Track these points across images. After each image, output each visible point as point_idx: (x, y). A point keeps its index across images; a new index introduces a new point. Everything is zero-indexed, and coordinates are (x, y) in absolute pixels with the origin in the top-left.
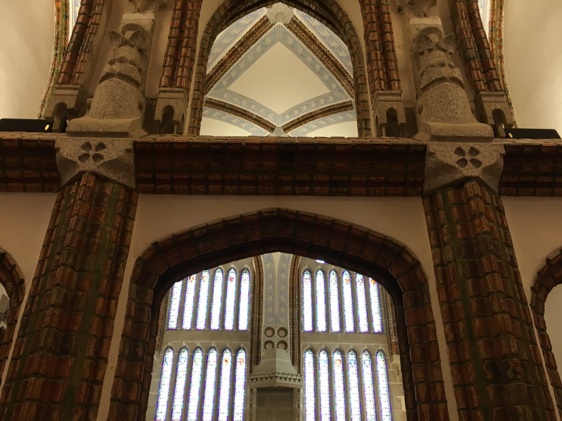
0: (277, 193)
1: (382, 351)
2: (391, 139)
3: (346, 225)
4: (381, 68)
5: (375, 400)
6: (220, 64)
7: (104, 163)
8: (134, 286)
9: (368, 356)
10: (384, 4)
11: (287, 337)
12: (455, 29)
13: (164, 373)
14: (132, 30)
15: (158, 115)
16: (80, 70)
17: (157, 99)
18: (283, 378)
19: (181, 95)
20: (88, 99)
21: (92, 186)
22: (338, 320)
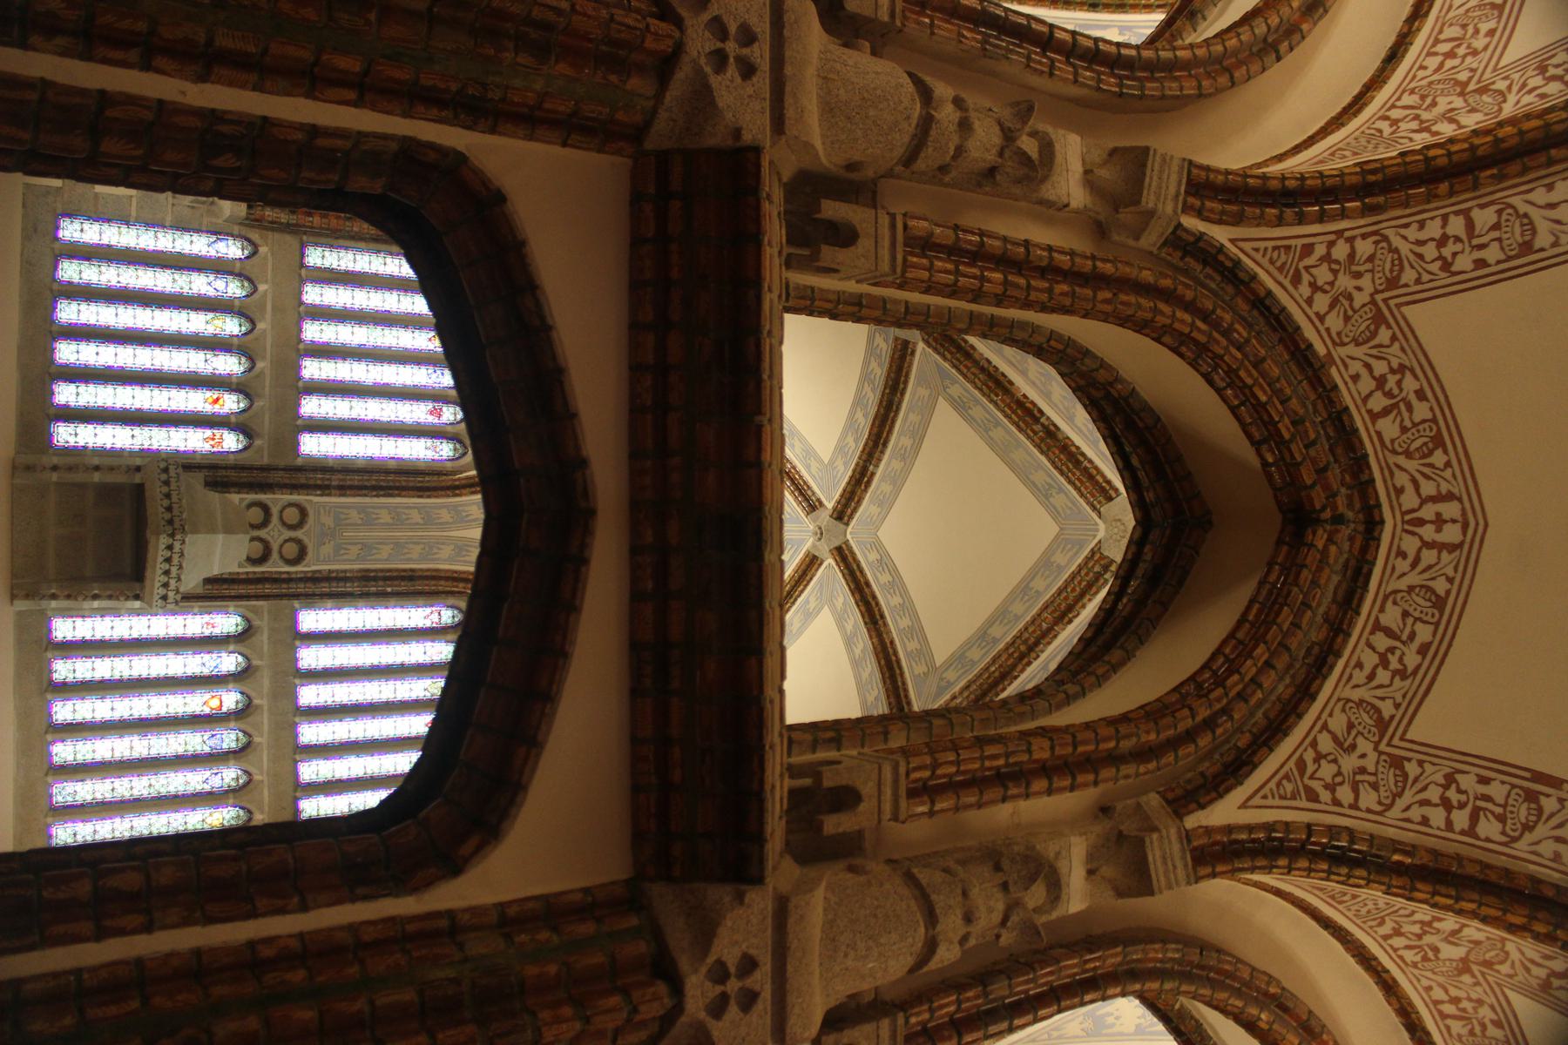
0: (636, 507)
2: (781, 799)
3: (554, 687)
4: (962, 768)
5: (116, 802)
6: (1002, 378)
7: (705, 76)
8: (394, 146)
9: (233, 784)
10: (1118, 770)
11: (281, 563)
12: (1061, 946)
13: (187, 237)
14: (1040, 152)
15: (832, 209)
16: (939, 27)
17: (875, 207)
18: (169, 554)
19: (885, 266)
20: (867, 44)
21: (647, 45)
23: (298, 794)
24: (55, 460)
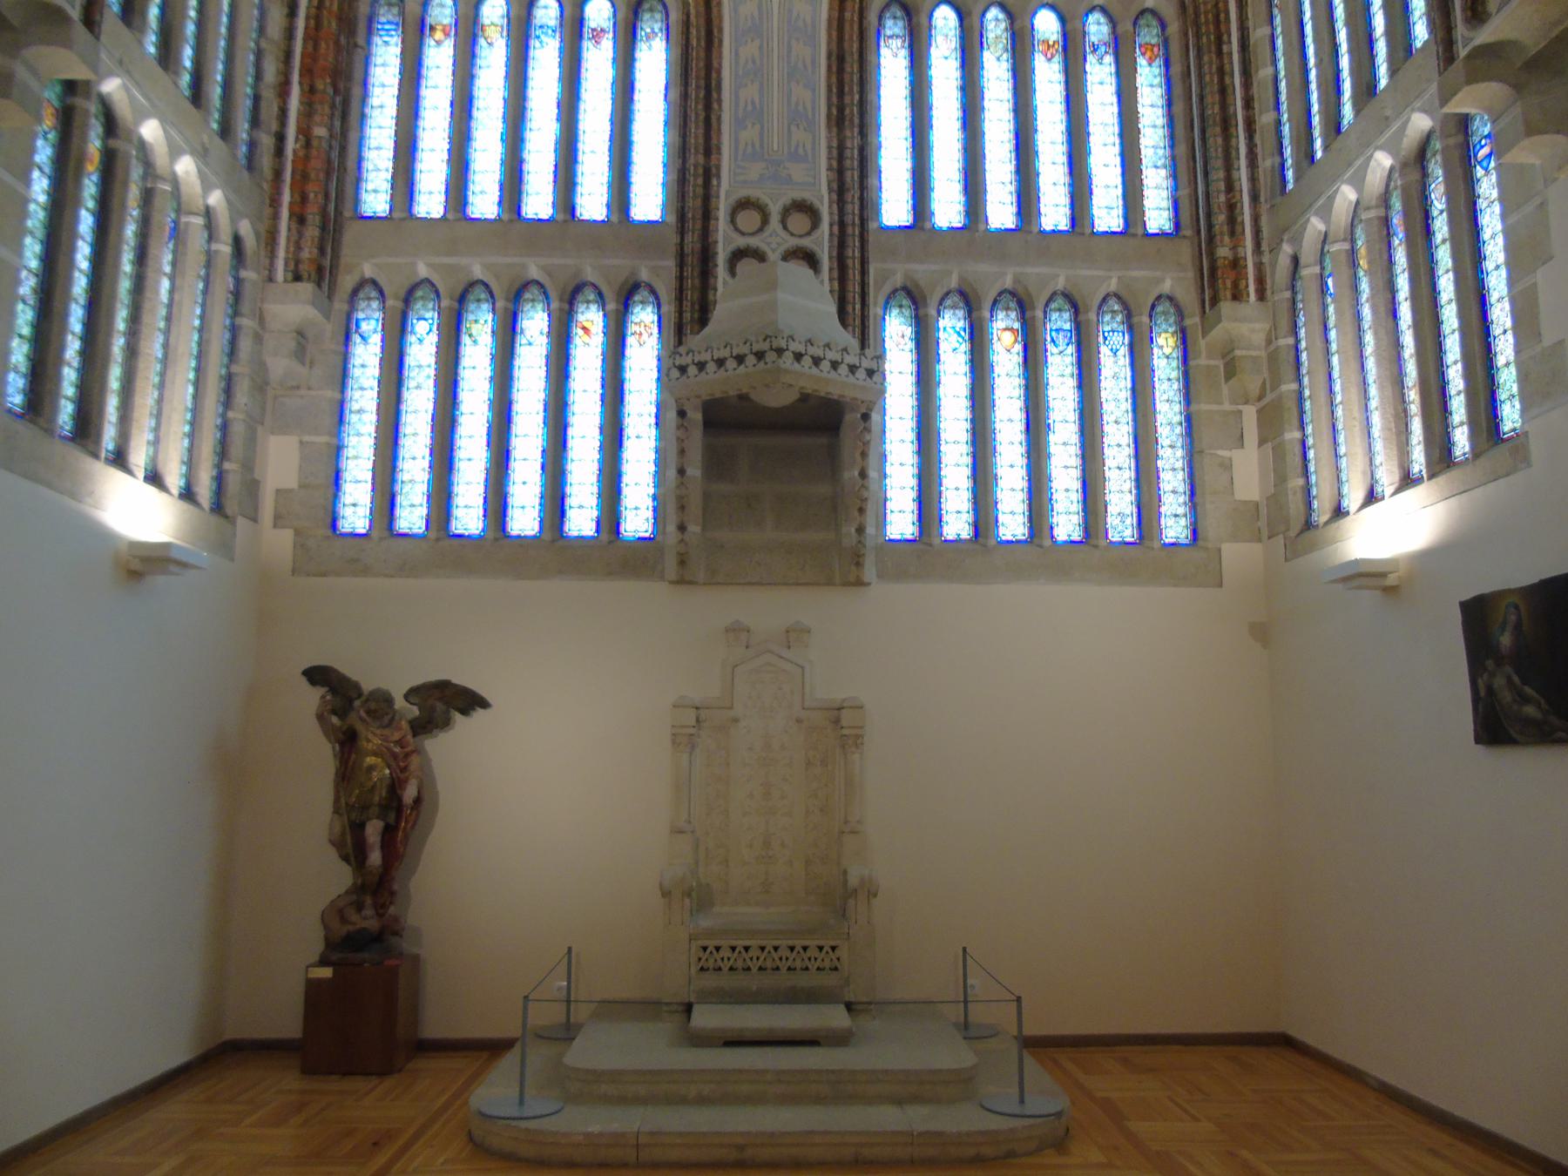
9: (1119, 318)
13: (356, 372)
18: (805, 358)
22: (1012, 188)
23: (1140, 231)
24: (671, 528)
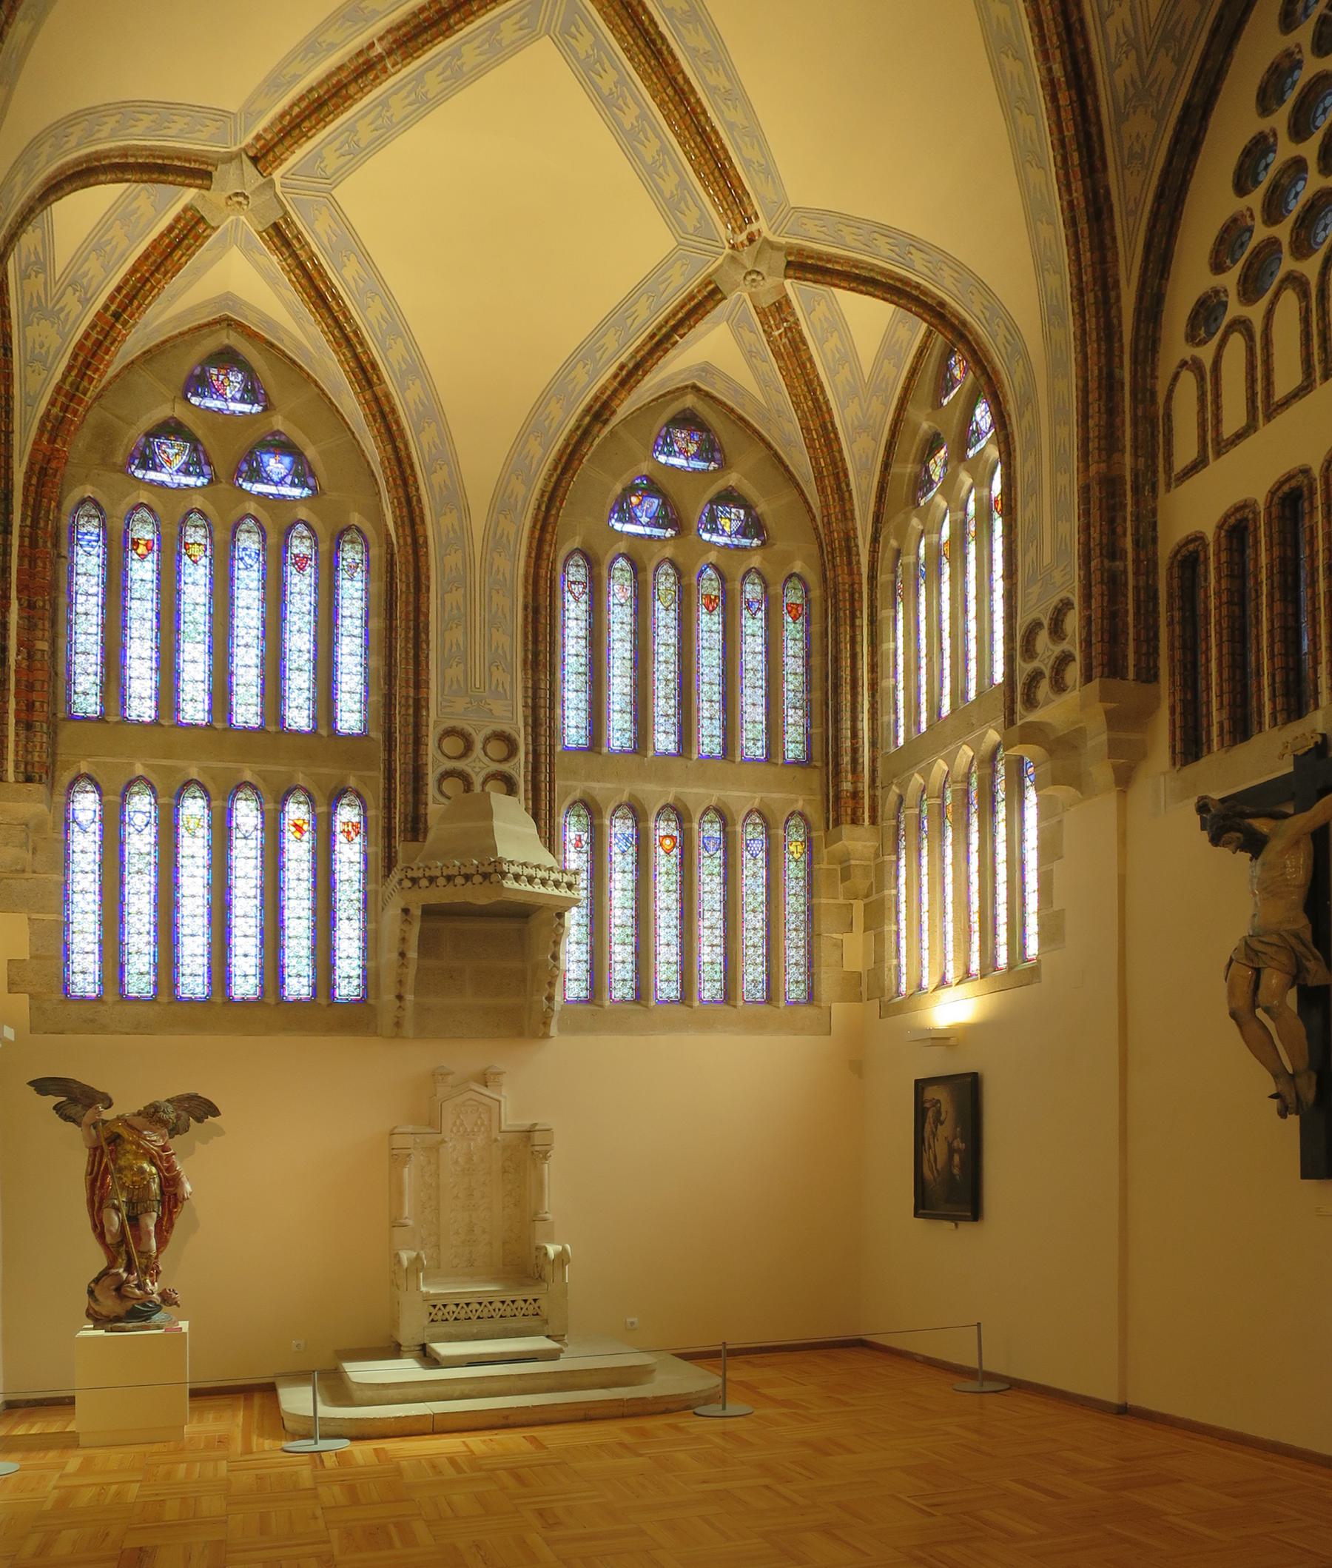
1: (801, 814)
